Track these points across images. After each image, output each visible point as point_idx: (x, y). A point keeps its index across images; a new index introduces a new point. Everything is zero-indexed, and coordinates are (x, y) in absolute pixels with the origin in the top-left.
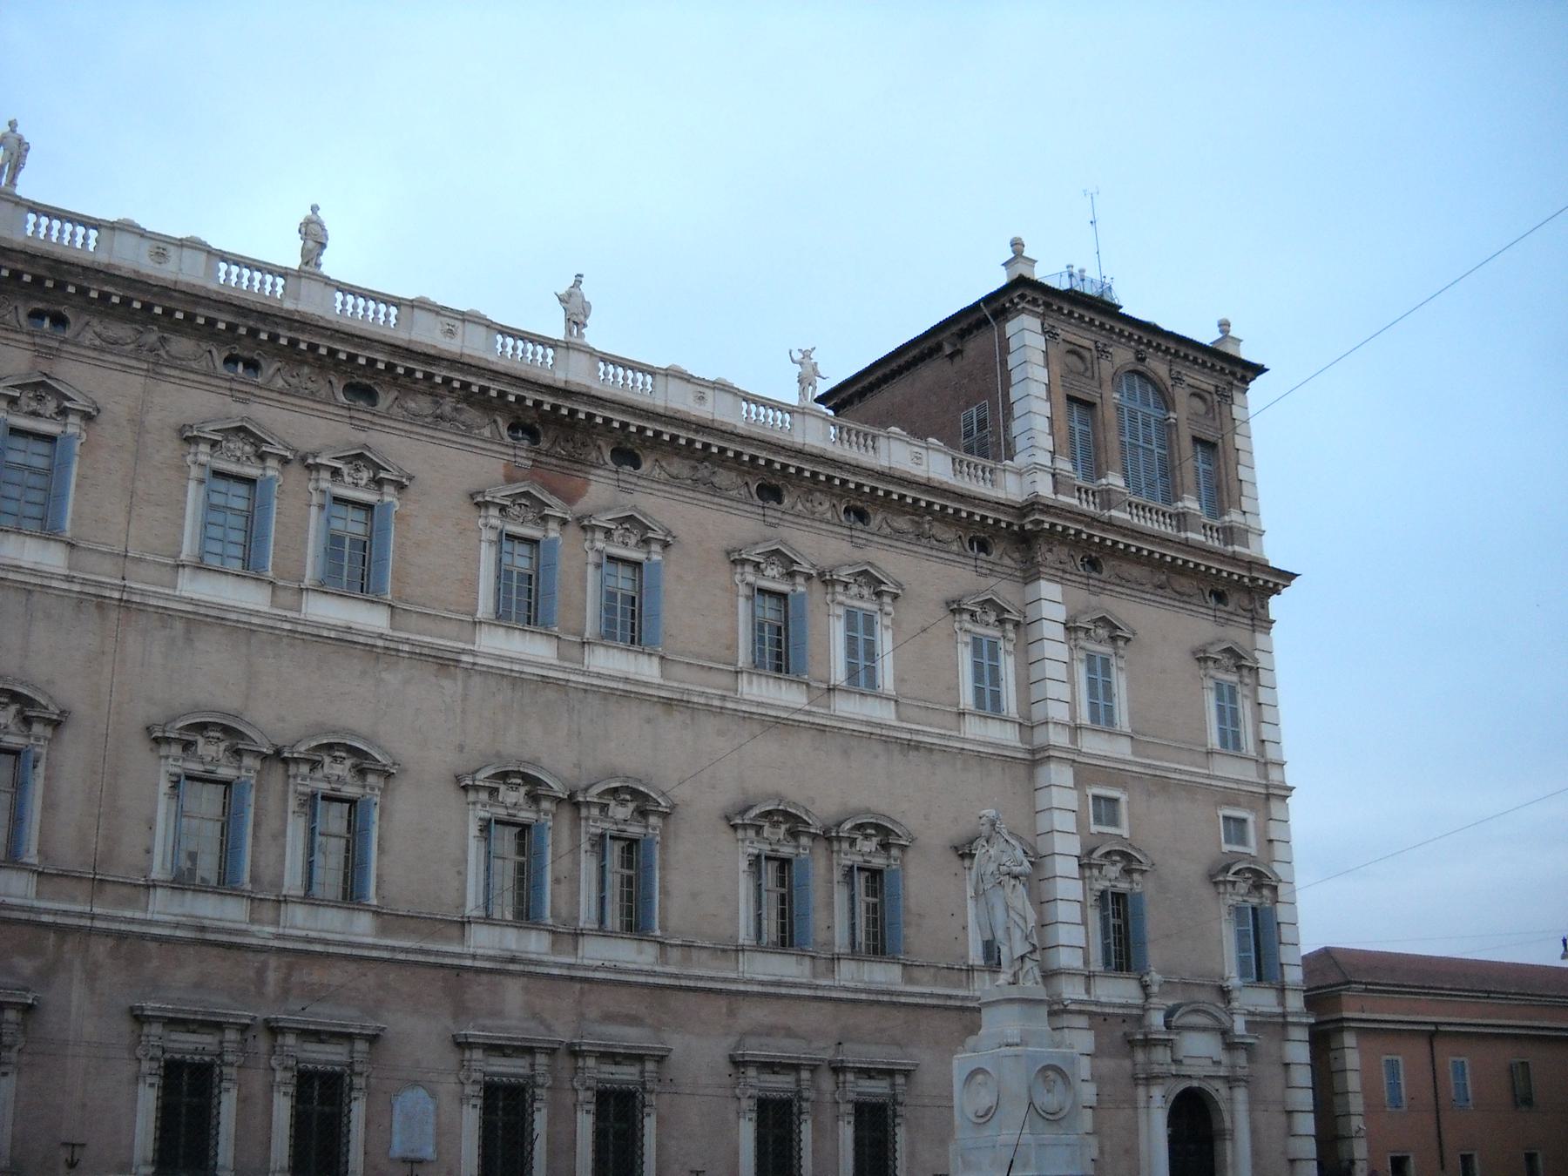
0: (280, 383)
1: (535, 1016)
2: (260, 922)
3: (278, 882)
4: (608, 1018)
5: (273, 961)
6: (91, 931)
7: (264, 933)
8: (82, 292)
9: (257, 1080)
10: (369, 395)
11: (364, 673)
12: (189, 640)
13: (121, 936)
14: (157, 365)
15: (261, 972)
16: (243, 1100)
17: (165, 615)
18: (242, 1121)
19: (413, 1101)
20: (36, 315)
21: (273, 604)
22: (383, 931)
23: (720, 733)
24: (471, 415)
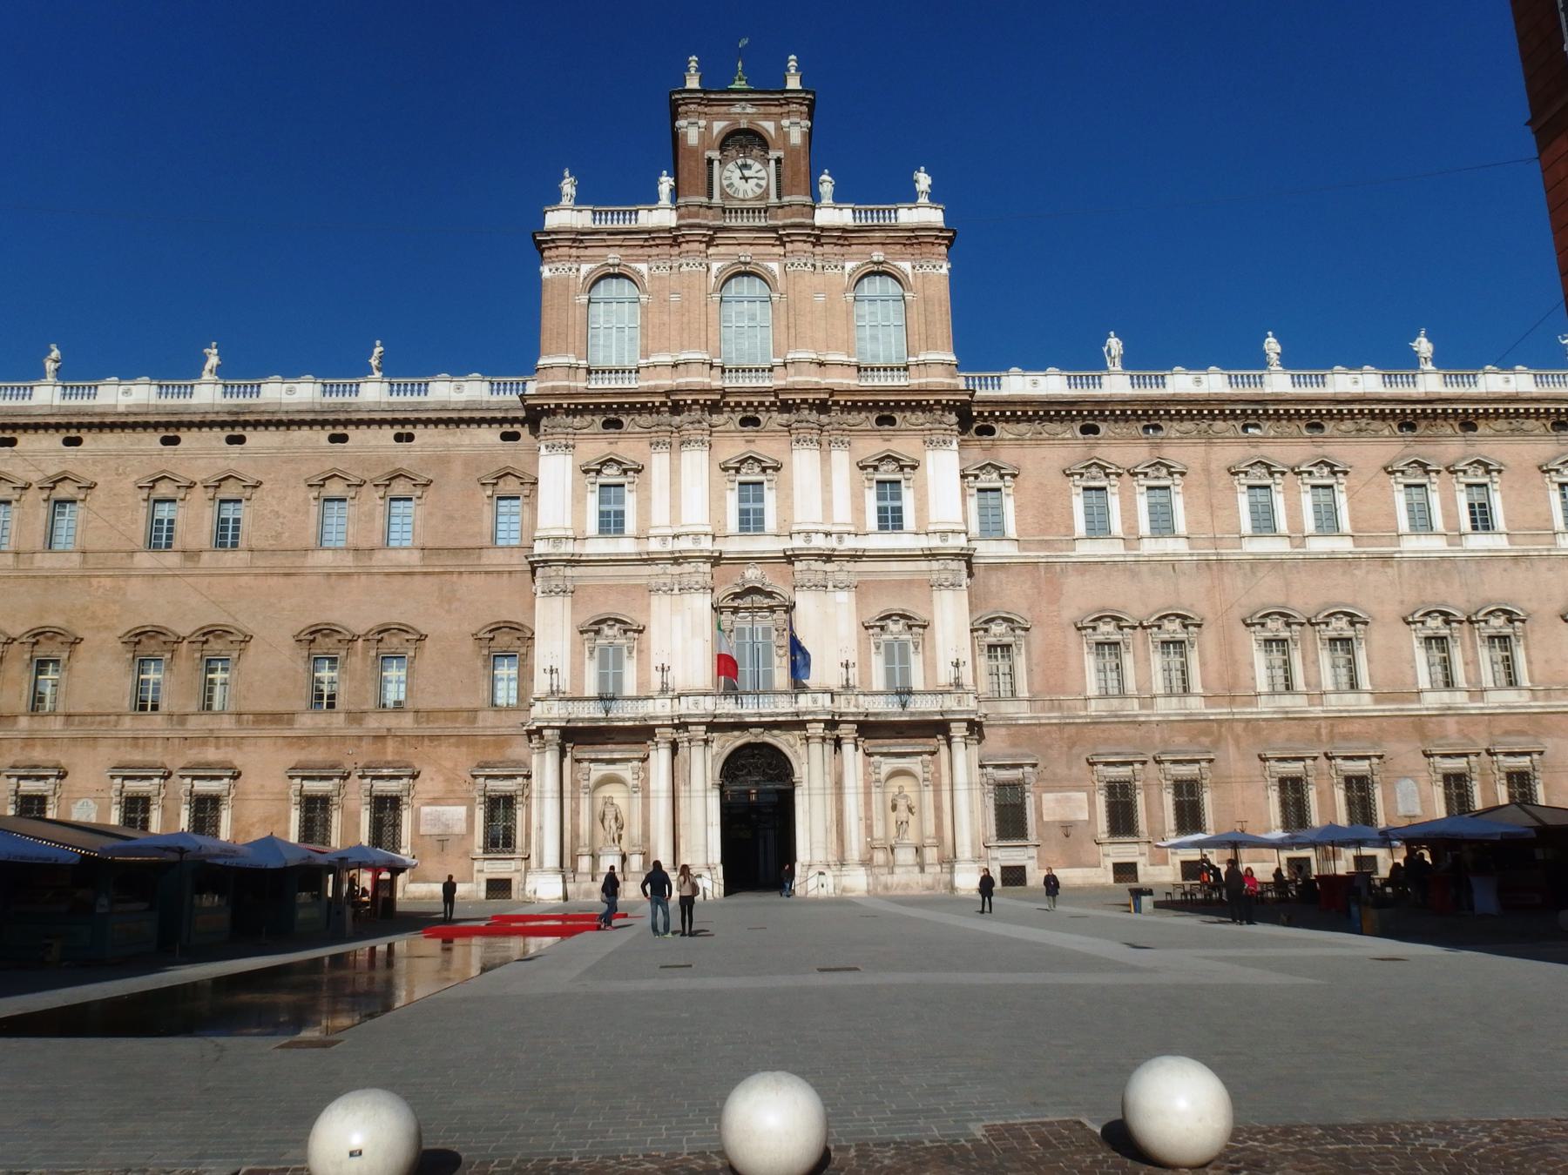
0: (1272, 433)
1: (1465, 736)
3: (1319, 684)
4: (1507, 733)
5: (1323, 723)
6: (1233, 720)
7: (1317, 711)
8: (1167, 412)
9: (1325, 785)
10: (1319, 427)
11: (1344, 573)
12: (1253, 572)
13: (1248, 720)
14: (1209, 439)
15: (1318, 729)
16: (1319, 793)
17: (1239, 563)
19: (1405, 787)
20: (1146, 428)
21: (1292, 546)
22: (1377, 702)
23: (1550, 569)
24: (1377, 424)
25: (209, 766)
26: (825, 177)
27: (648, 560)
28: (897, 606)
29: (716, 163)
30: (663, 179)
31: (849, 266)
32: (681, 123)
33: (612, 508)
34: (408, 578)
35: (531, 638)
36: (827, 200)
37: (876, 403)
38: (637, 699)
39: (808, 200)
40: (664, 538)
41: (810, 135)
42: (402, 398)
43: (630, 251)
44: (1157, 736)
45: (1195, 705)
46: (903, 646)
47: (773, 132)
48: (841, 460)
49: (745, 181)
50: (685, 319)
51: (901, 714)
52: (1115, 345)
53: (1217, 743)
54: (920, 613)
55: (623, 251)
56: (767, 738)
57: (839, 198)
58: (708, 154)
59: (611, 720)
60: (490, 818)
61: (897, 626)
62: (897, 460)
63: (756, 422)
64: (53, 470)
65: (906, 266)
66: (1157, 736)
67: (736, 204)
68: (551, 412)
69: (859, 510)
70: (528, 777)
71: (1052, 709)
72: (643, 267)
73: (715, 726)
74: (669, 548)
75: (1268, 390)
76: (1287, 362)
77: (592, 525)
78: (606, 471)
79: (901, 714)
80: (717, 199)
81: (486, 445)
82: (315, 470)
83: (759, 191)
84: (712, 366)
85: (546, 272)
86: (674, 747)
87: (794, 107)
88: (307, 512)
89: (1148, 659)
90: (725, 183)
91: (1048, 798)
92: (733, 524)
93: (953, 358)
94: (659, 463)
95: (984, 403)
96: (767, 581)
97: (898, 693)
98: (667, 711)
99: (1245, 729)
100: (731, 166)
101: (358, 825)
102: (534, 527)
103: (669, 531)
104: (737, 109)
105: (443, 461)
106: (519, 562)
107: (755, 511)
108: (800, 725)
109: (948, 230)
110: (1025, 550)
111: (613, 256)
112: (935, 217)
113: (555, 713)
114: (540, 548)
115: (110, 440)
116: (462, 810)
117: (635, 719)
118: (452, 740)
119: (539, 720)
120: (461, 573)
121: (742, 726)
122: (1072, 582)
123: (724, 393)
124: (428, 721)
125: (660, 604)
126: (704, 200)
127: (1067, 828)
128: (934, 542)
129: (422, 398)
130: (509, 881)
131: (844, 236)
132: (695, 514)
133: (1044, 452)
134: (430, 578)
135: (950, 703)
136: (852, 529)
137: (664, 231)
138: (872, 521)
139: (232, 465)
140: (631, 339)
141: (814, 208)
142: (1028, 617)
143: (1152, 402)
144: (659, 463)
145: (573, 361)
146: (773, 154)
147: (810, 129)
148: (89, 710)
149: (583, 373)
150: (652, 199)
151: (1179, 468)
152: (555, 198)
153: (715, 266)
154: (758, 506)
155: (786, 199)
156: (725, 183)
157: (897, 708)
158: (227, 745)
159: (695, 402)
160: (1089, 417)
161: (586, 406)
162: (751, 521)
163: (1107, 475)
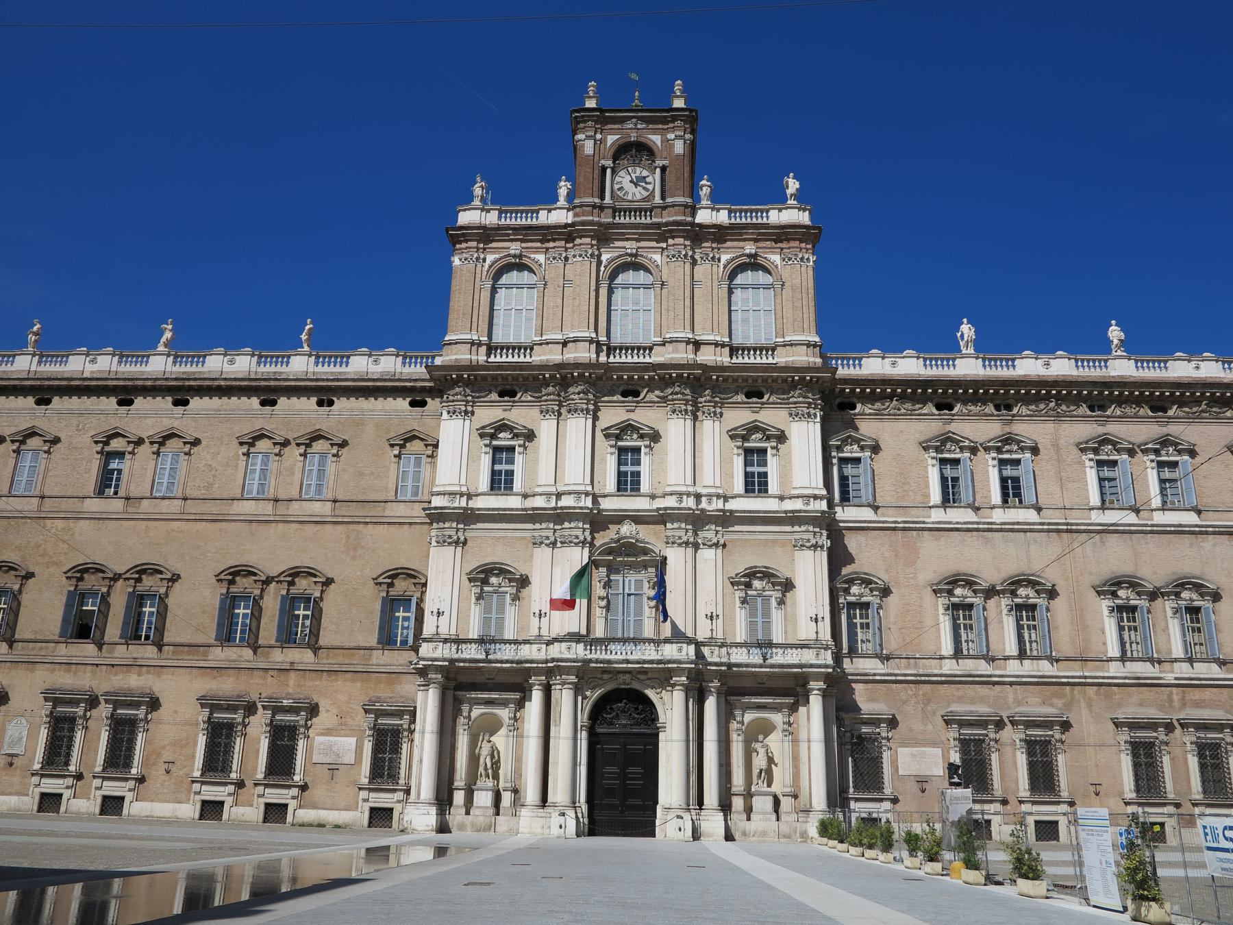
2: (1165, 672)
7: (1169, 678)
11: (1191, 545)
14: (1058, 418)
15: (1170, 696)
16: (1172, 759)
18: (1173, 769)
25: (129, 692)
26: (704, 182)
27: (533, 516)
28: (760, 562)
29: (609, 171)
30: (562, 183)
31: (725, 258)
32: (580, 136)
33: (503, 467)
34: (319, 527)
35: (425, 585)
36: (704, 202)
37: (745, 380)
38: (516, 642)
39: (689, 200)
40: (549, 495)
41: (692, 148)
42: (326, 369)
43: (530, 244)
44: (1011, 696)
45: (1045, 668)
46: (767, 600)
47: (659, 143)
50: (577, 302)
51: (761, 666)
52: (967, 330)
53: (1069, 705)
55: (524, 245)
56: (636, 686)
57: (717, 199)
58: (603, 162)
59: (490, 662)
60: (377, 749)
61: (761, 584)
62: (764, 430)
64: (24, 425)
65: (776, 258)
66: (1011, 696)
67: (625, 205)
68: (455, 383)
69: (727, 474)
70: (413, 714)
71: (908, 667)
72: (541, 258)
74: (553, 504)
75: (1113, 374)
76: (1132, 348)
77: (484, 484)
78: (501, 435)
79: (761, 666)
80: (608, 200)
81: (397, 411)
82: (247, 427)
83: (646, 194)
84: (599, 345)
85: (456, 261)
87: (678, 123)
88: (237, 466)
89: (1001, 622)
90: (616, 187)
91: (904, 753)
93: (817, 339)
94: (546, 429)
95: (846, 381)
96: (641, 536)
97: (759, 645)
98: (542, 656)
99: (1097, 693)
100: (622, 173)
101: (258, 751)
102: (433, 483)
103: (553, 489)
105: (358, 423)
106: (417, 511)
107: (633, 473)
108: (663, 676)
109: (814, 228)
110: (883, 515)
111: (515, 248)
112: (804, 218)
113: (438, 654)
114: (437, 502)
115: (74, 402)
116: (352, 741)
117: (512, 662)
118: (349, 675)
119: (424, 659)
120: (367, 523)
121: (608, 671)
122: (927, 544)
123: (608, 367)
124: (328, 657)
125: (543, 553)
126: (597, 200)
127: (922, 782)
128: (798, 505)
129: (344, 369)
130: (391, 810)
131: (720, 234)
132: (575, 474)
133: (902, 425)
134: (339, 527)
135: (808, 656)
136: (721, 491)
137: (560, 227)
138: (739, 486)
139: (176, 424)
140: (528, 319)
141: (693, 210)
142: (886, 578)
143: (1006, 383)
144: (546, 429)
145: (475, 337)
146: (659, 163)
147: (693, 142)
148: (32, 637)
149: (483, 349)
150: (550, 199)
151: (1029, 443)
152: (466, 199)
153: (605, 257)
154: (635, 469)
155: (669, 200)
156: (616, 187)
157: (757, 659)
158: (148, 672)
160: (944, 396)
161: (484, 378)
162: (628, 483)
163: (962, 449)
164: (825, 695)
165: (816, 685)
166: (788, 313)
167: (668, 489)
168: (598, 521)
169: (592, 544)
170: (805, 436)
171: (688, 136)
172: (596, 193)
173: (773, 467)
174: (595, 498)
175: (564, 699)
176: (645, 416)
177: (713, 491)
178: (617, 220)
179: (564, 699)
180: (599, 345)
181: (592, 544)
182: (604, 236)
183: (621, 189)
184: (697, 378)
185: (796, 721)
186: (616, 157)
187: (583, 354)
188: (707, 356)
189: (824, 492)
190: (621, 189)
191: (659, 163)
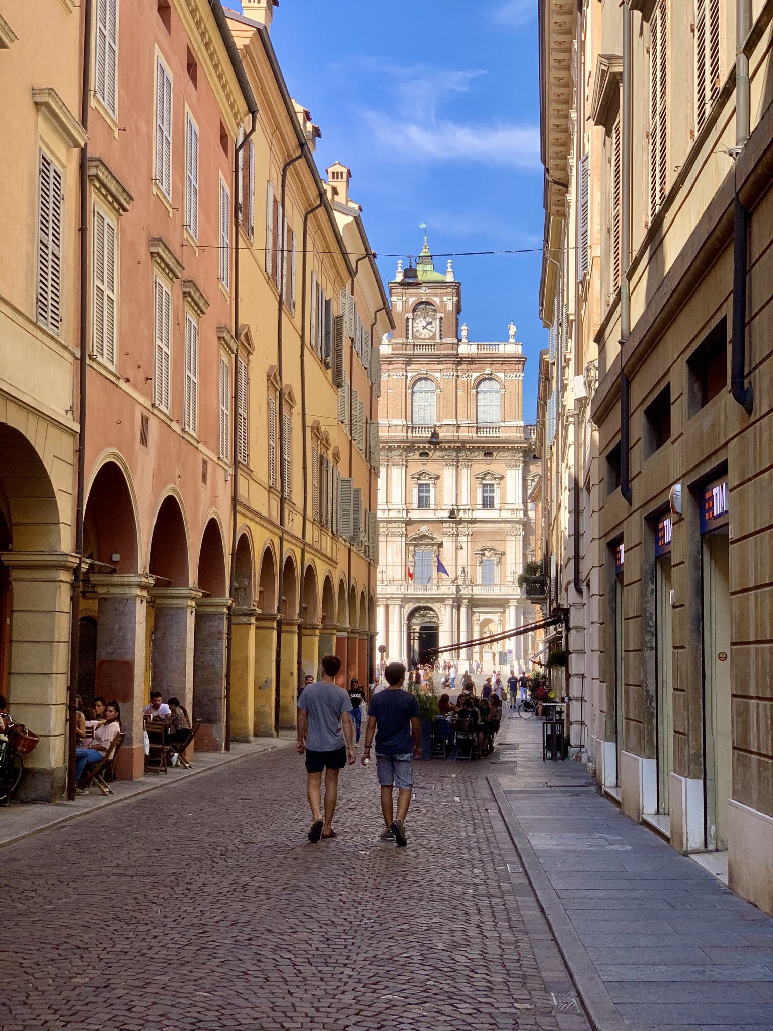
26: (464, 327)
29: (410, 320)
36: (464, 341)
39: (455, 341)
40: (384, 510)
47: (438, 302)
48: (465, 472)
49: (423, 329)
54: (500, 549)
58: (407, 315)
63: (426, 454)
65: (501, 375)
69: (473, 498)
73: (405, 600)
80: (410, 341)
84: (407, 427)
86: (387, 607)
87: (449, 290)
92: (415, 506)
100: (417, 321)
103: (386, 507)
104: (422, 291)
131: (472, 360)
136: (470, 507)
141: (458, 345)
147: (459, 302)
153: (410, 375)
155: (445, 340)
156: (415, 330)
159: (399, 446)
162: (423, 503)
164: (517, 608)
165: (513, 603)
166: (507, 407)
167: (444, 507)
168: (409, 522)
169: (406, 535)
170: (513, 478)
171: (455, 298)
172: (404, 335)
173: (497, 494)
174: (407, 512)
175: (395, 611)
176: (431, 467)
177: (466, 507)
178: (416, 352)
179: (395, 611)
180: (407, 427)
181: (406, 535)
182: (408, 361)
183: (417, 331)
184: (459, 447)
185: (504, 619)
186: (414, 312)
187: (400, 434)
188: (464, 434)
189: (522, 507)
190: (417, 331)
191: (439, 315)
